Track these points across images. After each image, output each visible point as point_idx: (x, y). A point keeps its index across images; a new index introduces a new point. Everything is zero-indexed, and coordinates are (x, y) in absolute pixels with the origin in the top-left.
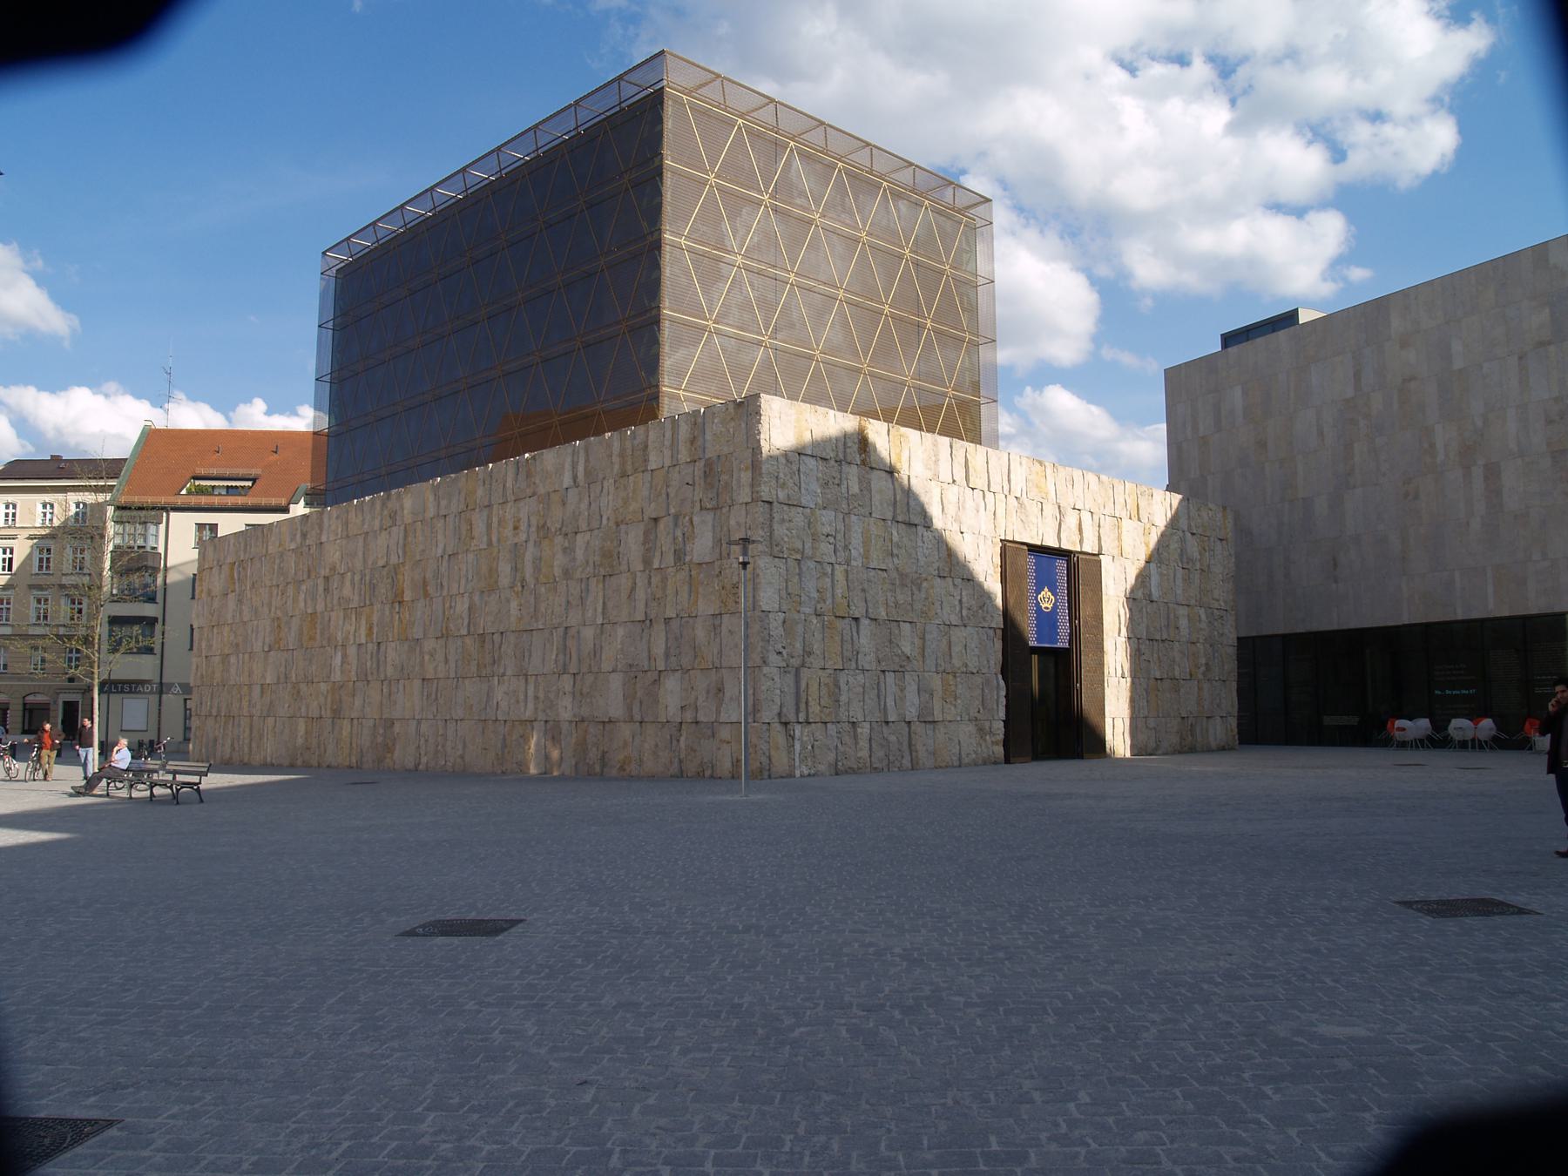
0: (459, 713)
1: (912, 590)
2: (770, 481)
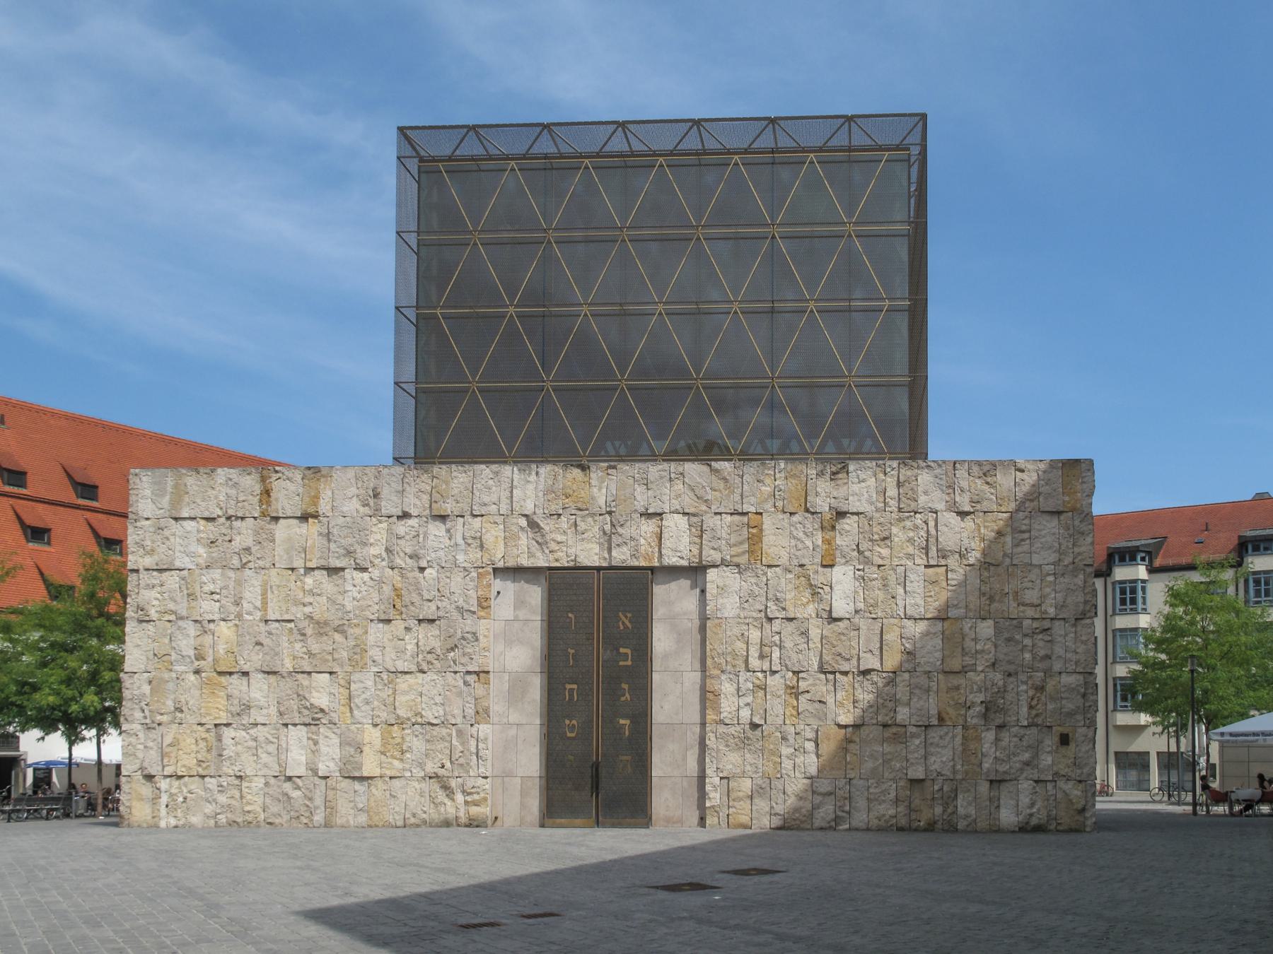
2: (138, 551)
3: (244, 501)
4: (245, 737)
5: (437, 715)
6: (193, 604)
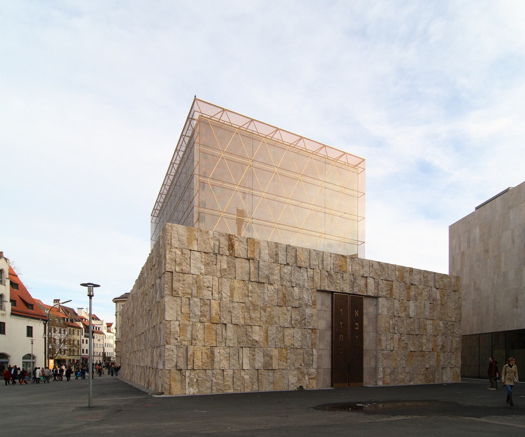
1: (260, 312)
3: (222, 248)
4: (223, 353)
5: (299, 345)
6: (200, 291)
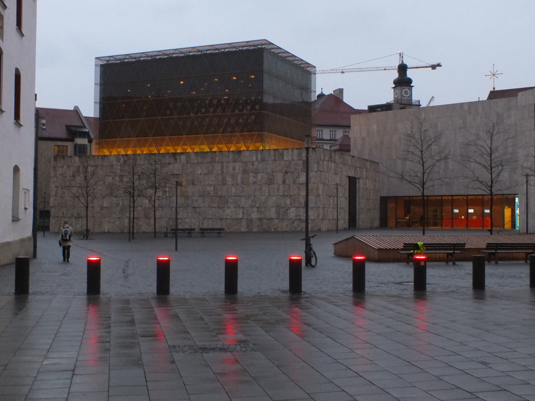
0: (211, 217)
